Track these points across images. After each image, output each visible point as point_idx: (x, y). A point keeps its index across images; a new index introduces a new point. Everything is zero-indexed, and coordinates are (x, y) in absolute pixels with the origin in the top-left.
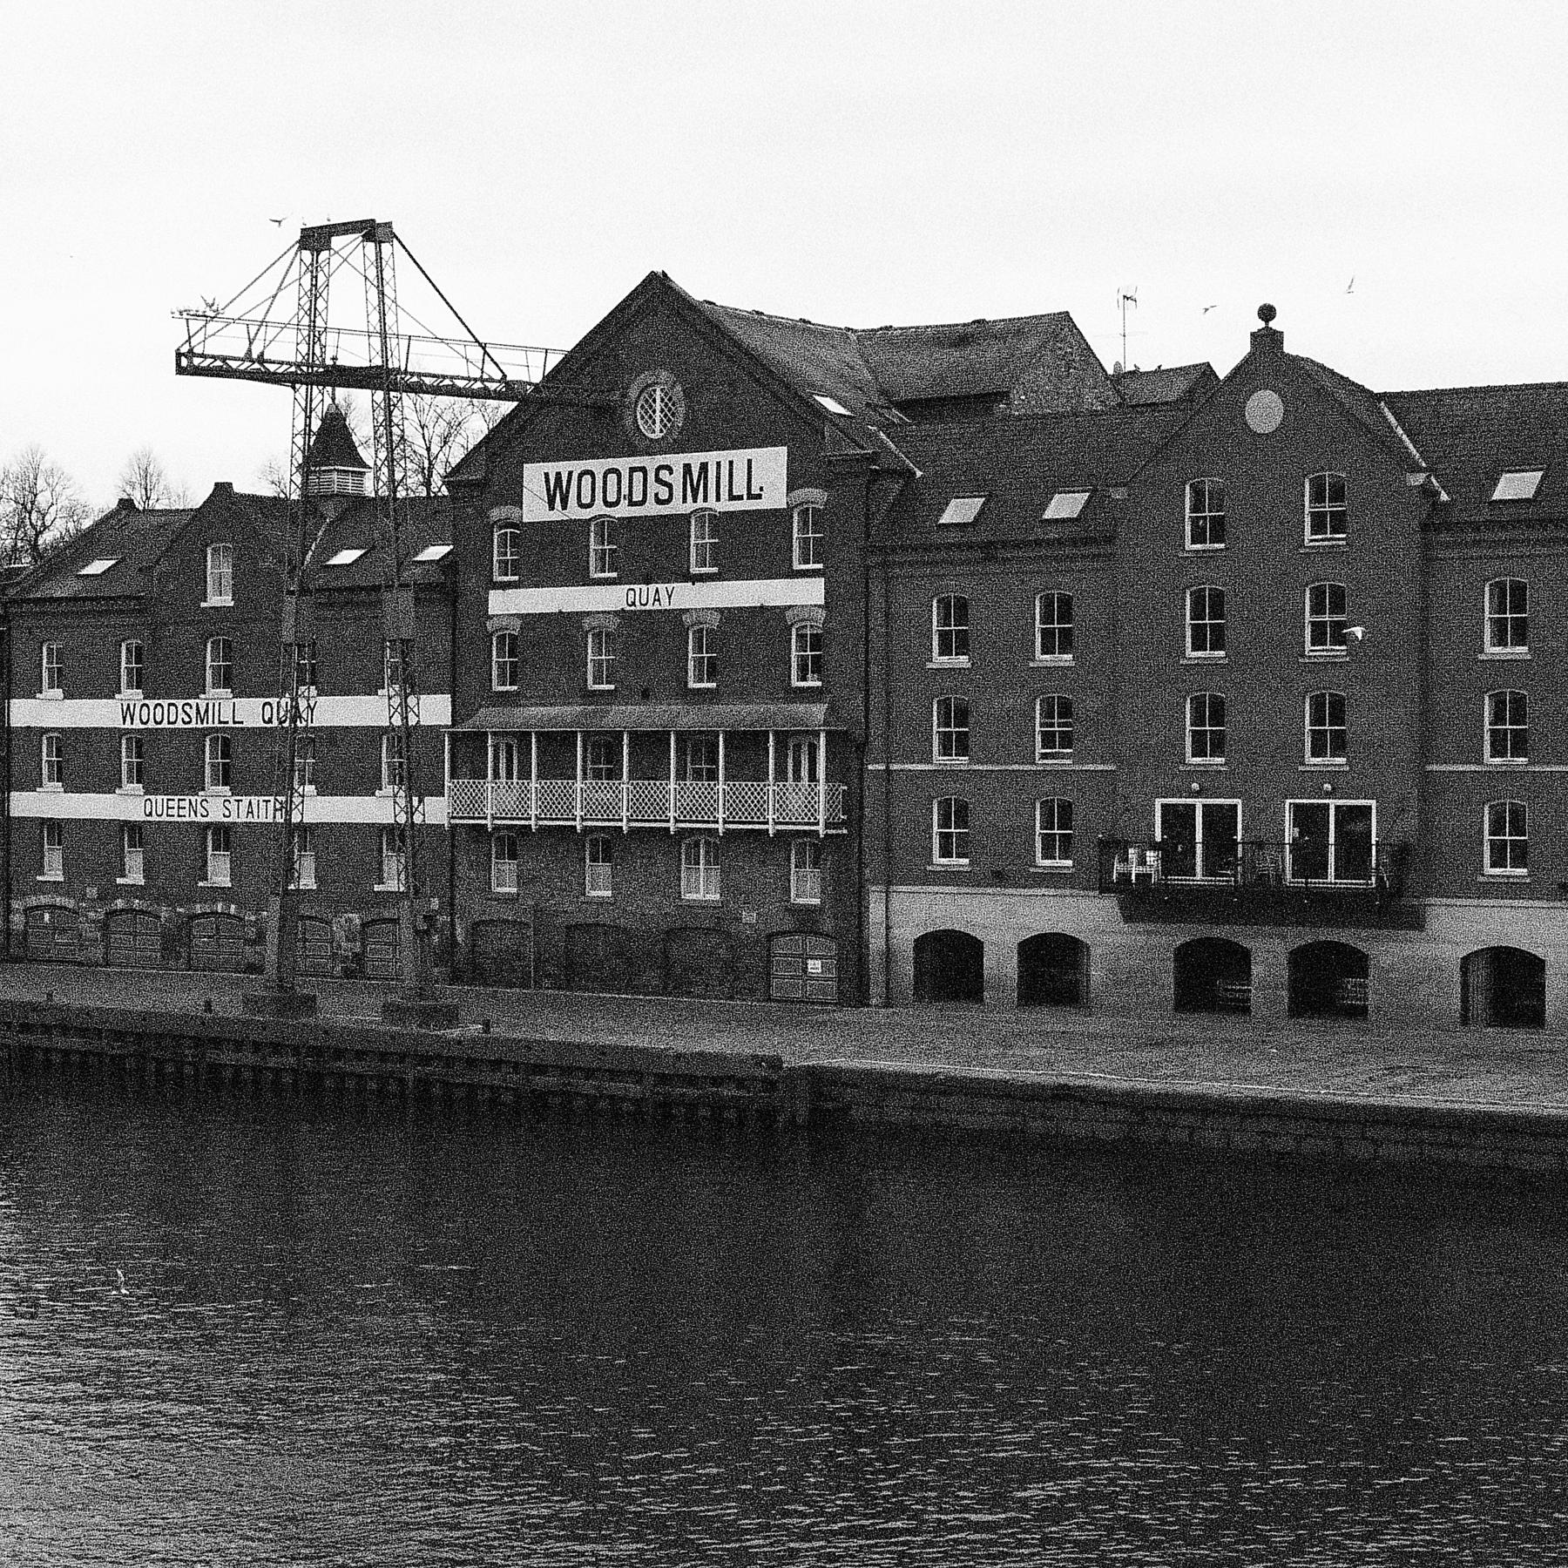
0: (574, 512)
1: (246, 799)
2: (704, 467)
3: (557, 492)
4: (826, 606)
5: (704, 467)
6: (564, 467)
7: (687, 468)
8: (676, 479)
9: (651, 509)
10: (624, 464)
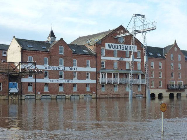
0: (112, 49)
1: (66, 80)
2: (128, 46)
3: (110, 46)
4: (141, 62)
5: (128, 46)
6: (111, 44)
7: (126, 46)
8: (124, 47)
9: (121, 50)
10: (118, 45)
